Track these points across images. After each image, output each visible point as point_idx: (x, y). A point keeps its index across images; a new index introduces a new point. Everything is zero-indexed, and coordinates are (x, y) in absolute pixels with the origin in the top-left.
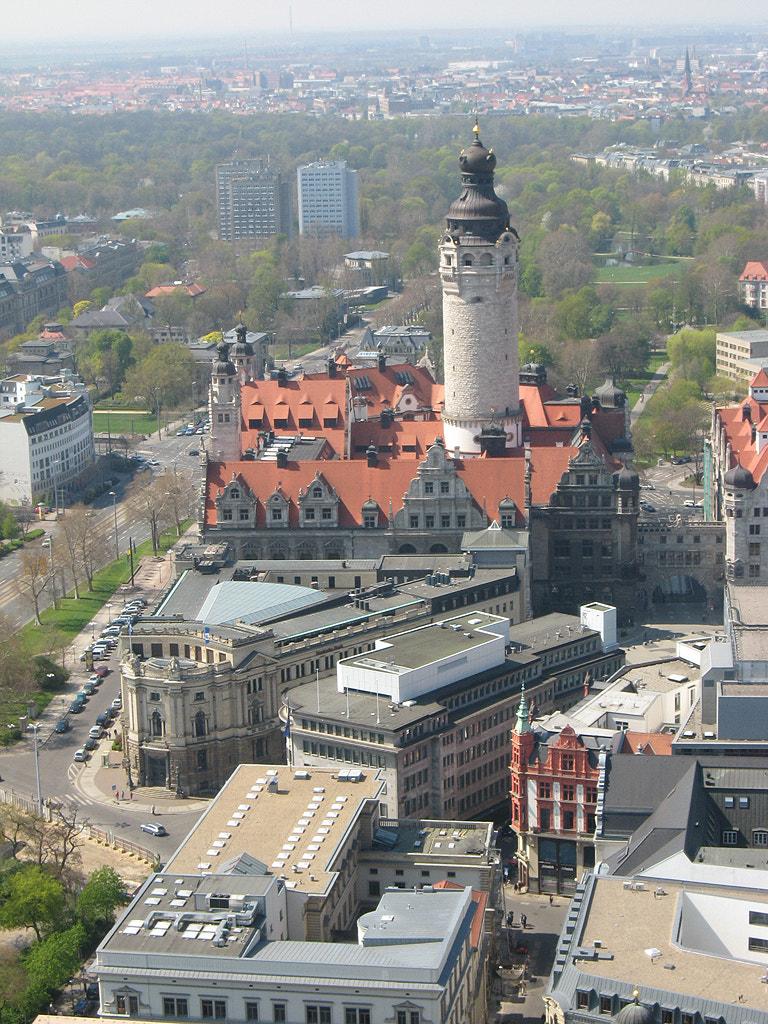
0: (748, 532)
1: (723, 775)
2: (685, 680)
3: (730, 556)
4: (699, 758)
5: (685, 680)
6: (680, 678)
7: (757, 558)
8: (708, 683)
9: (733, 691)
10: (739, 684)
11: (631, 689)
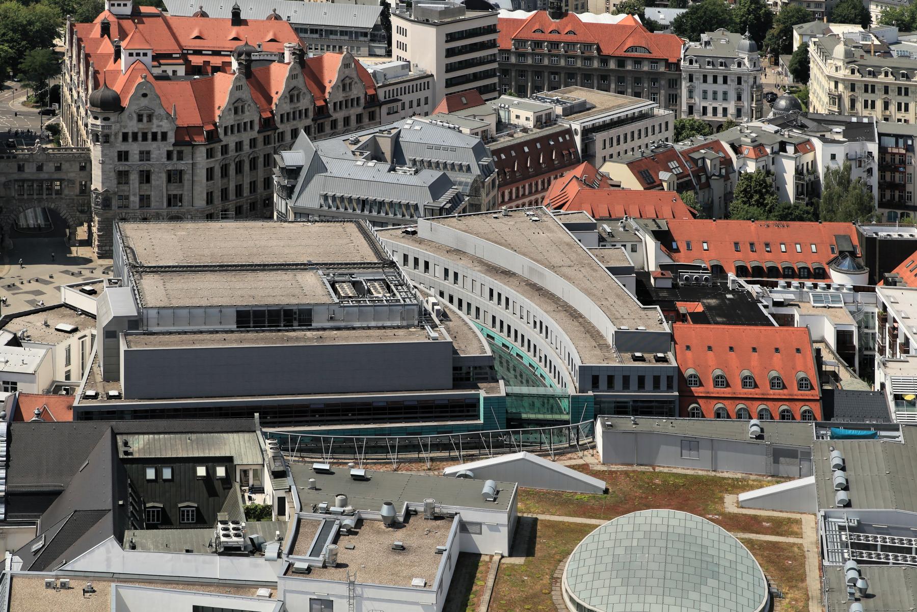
0: (116, 159)
1: (141, 442)
2: (75, 330)
3: (97, 184)
4: (113, 423)
5: (75, 330)
6: (69, 328)
7: (125, 187)
8: (110, 334)
9: (142, 344)
10: (144, 334)
11: (15, 342)
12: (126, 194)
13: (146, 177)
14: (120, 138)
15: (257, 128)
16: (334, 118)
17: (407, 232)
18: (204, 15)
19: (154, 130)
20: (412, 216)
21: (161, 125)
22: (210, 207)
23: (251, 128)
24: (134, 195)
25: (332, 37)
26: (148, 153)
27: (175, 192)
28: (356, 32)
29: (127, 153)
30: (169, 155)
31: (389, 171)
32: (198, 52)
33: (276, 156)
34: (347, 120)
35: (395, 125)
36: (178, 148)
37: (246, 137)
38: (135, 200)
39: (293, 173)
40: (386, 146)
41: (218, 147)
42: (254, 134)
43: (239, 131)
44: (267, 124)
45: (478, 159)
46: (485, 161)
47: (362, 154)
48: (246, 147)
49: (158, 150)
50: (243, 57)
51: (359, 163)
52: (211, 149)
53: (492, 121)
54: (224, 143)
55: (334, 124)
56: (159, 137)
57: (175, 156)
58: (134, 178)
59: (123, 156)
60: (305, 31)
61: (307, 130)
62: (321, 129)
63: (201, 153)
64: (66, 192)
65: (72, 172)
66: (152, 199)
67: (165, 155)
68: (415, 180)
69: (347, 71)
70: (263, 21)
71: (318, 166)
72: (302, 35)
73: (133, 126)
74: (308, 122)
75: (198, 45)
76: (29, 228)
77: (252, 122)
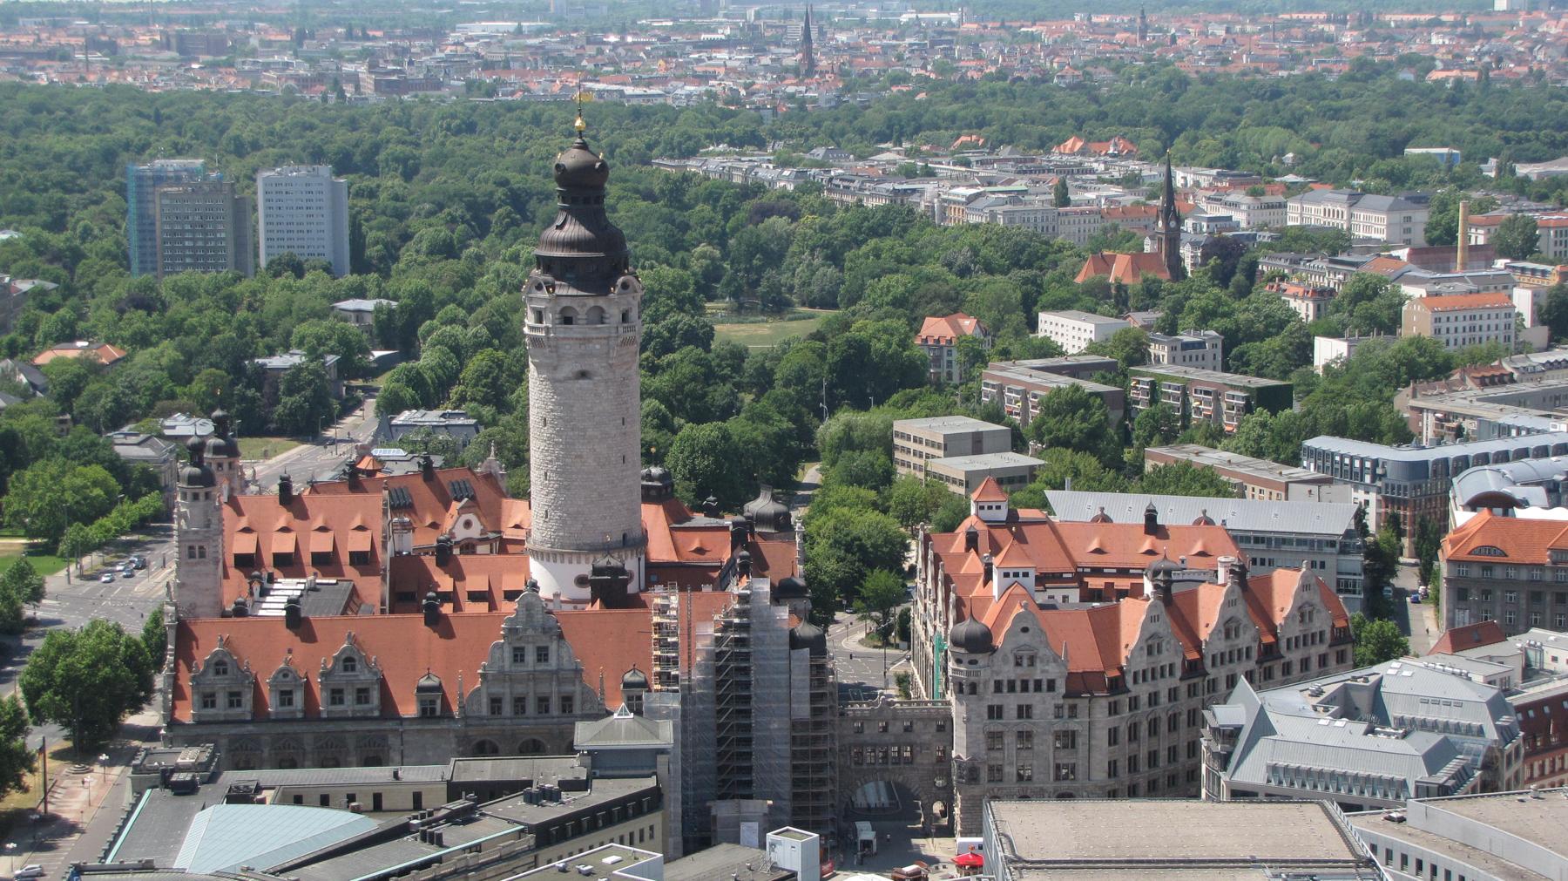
3: (959, 751)
14: (992, 688)
15: (1178, 674)
17: (1390, 819)
18: (1106, 519)
20: (1398, 797)
21: (1046, 670)
22: (1112, 781)
23: (1171, 673)
25: (1284, 547)
26: (1029, 707)
28: (1320, 542)
29: (1000, 708)
31: (1366, 733)
32: (1097, 572)
33: (1205, 713)
34: (1305, 664)
35: (1375, 669)
36: (1071, 701)
37: (1163, 686)
39: (1230, 735)
40: (1362, 701)
41: (1124, 699)
42: (1174, 682)
43: (1153, 678)
44: (1193, 669)
45: (1495, 717)
46: (1505, 720)
47: (1326, 710)
48: (1164, 698)
49: (1043, 704)
50: (1160, 577)
51: (1322, 722)
53: (1517, 666)
54: (1133, 694)
55: (1287, 669)
56: (1045, 686)
57: (1066, 712)
58: (1010, 740)
59: (995, 712)
60: (1247, 539)
61: (1250, 676)
62: (1268, 675)
63: (1101, 705)
64: (918, 759)
65: (926, 734)
67: (1052, 710)
68: (1404, 746)
69: (1306, 595)
70: (1187, 528)
71: (1263, 727)
72: (1243, 546)
73: (1009, 672)
74: (1251, 665)
75: (1097, 561)
76: (869, 808)
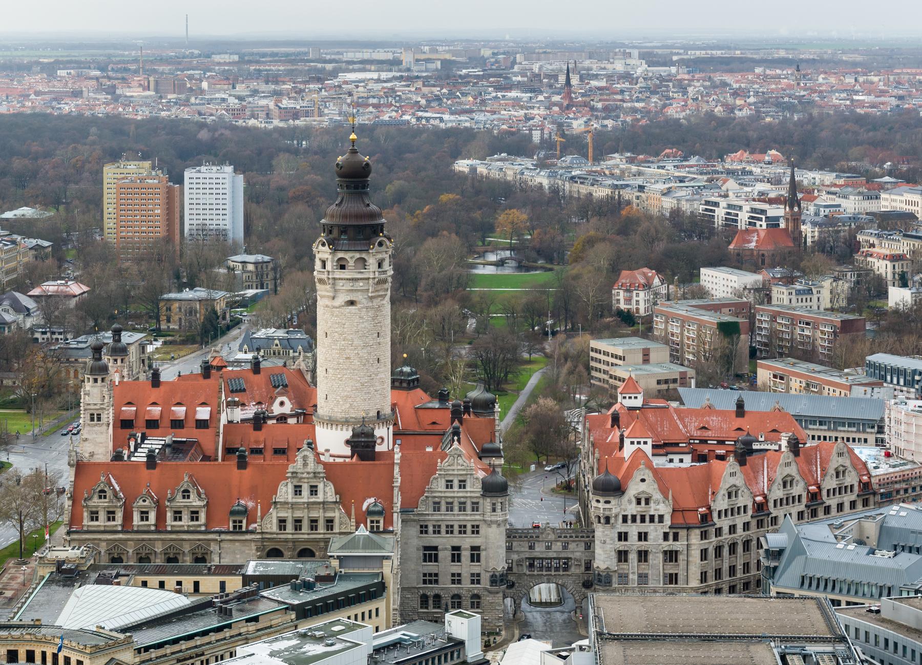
0: (617, 539)
7: (624, 566)
12: (626, 572)
13: (643, 556)
15: (750, 512)
16: (827, 504)
19: (652, 513)
24: (633, 573)
27: (671, 572)
30: (666, 536)
34: (840, 507)
36: (674, 531)
37: (740, 521)
38: (633, 577)
49: (655, 532)
52: (706, 531)
56: (656, 519)
57: (671, 537)
58: (633, 557)
66: (650, 577)
67: (661, 536)
73: (632, 509)
77: (745, 507)
